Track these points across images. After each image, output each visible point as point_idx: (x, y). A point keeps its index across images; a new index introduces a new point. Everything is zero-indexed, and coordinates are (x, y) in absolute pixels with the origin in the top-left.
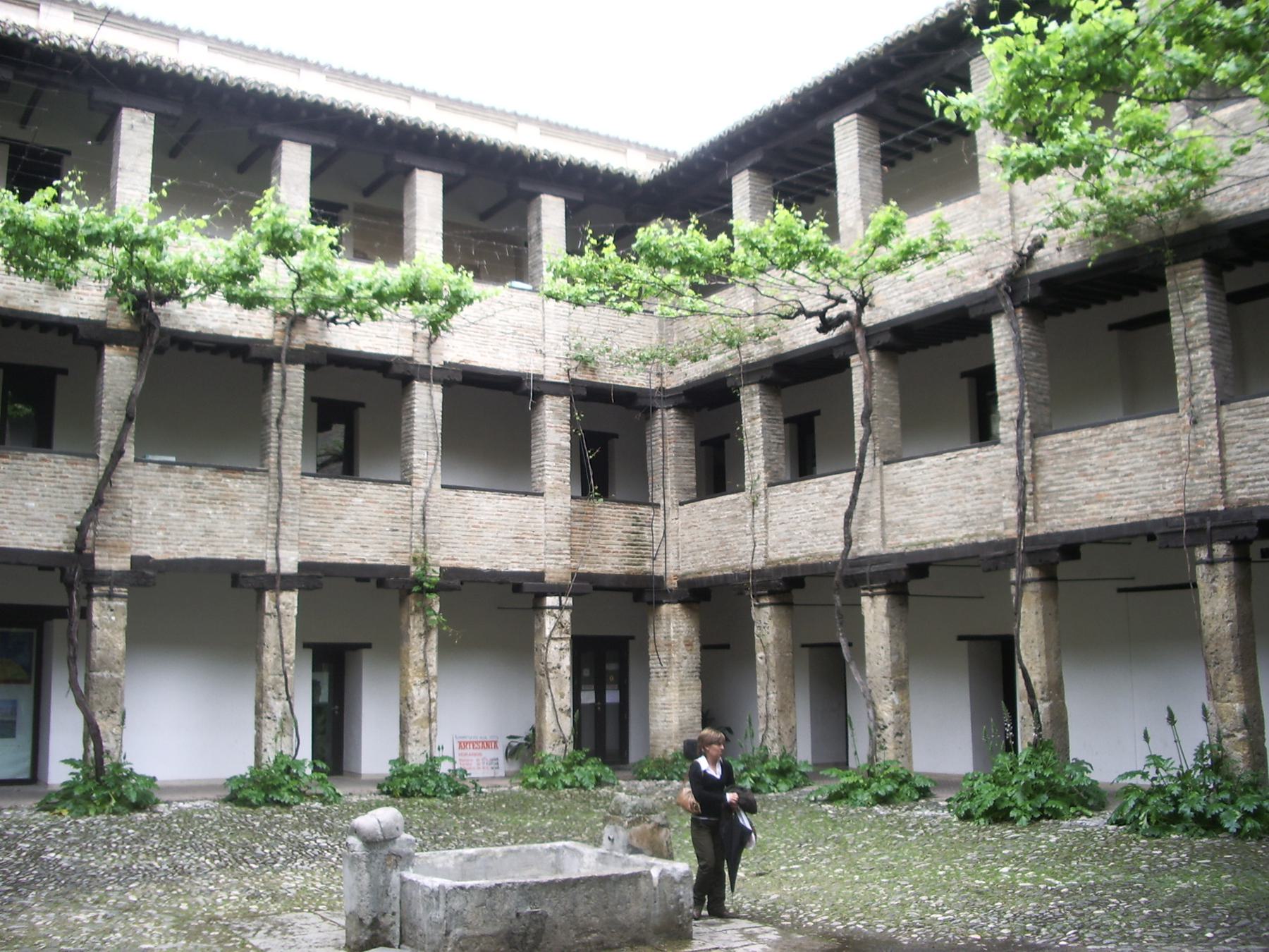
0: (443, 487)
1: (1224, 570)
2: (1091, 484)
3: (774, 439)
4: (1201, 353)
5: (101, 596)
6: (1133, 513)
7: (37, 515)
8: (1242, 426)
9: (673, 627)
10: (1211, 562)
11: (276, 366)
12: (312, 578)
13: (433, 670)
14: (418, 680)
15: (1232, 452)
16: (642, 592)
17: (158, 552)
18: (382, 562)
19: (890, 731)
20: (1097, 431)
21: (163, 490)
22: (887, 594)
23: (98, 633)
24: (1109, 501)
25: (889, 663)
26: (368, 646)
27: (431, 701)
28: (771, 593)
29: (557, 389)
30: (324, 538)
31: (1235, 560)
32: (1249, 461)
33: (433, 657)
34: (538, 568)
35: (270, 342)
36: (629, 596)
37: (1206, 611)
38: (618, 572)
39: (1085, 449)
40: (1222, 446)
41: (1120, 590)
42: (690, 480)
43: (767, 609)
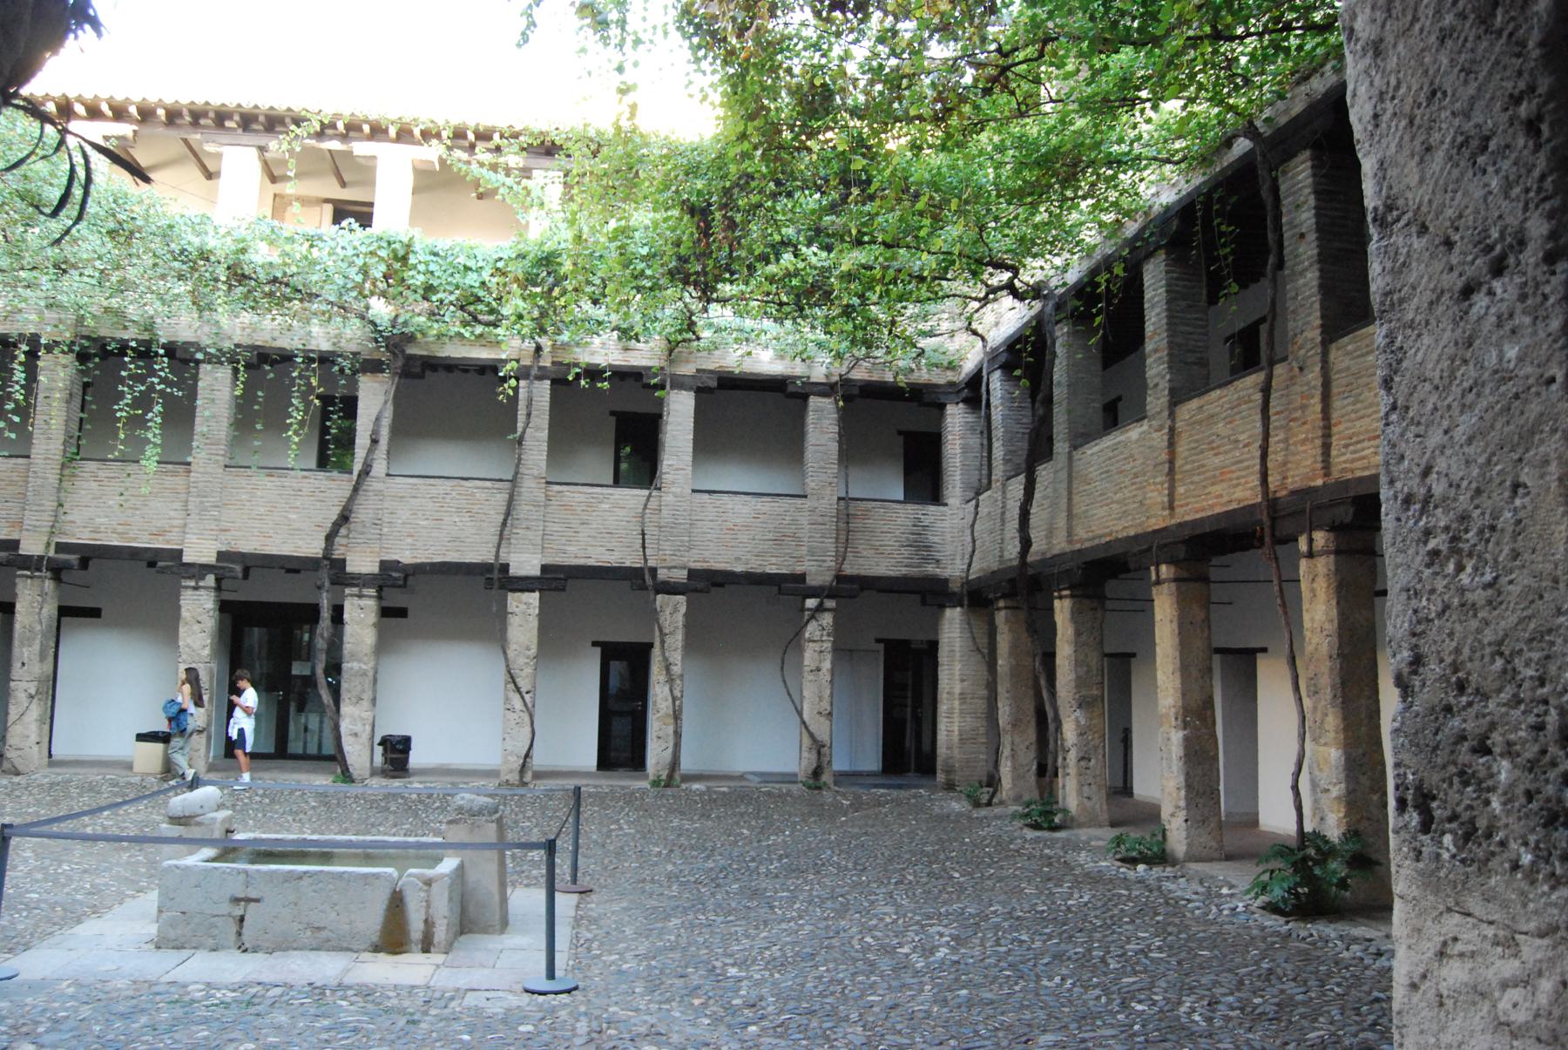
0: (694, 491)
3: (1018, 428)
7: (296, 525)
9: (953, 628)
13: (676, 669)
17: (407, 557)
18: (628, 564)
20: (1224, 391)
22: (1072, 596)
23: (349, 630)
25: (1072, 676)
27: (674, 699)
28: (1004, 596)
29: (827, 389)
31: (1337, 552)
33: (676, 657)
34: (799, 569)
36: (918, 597)
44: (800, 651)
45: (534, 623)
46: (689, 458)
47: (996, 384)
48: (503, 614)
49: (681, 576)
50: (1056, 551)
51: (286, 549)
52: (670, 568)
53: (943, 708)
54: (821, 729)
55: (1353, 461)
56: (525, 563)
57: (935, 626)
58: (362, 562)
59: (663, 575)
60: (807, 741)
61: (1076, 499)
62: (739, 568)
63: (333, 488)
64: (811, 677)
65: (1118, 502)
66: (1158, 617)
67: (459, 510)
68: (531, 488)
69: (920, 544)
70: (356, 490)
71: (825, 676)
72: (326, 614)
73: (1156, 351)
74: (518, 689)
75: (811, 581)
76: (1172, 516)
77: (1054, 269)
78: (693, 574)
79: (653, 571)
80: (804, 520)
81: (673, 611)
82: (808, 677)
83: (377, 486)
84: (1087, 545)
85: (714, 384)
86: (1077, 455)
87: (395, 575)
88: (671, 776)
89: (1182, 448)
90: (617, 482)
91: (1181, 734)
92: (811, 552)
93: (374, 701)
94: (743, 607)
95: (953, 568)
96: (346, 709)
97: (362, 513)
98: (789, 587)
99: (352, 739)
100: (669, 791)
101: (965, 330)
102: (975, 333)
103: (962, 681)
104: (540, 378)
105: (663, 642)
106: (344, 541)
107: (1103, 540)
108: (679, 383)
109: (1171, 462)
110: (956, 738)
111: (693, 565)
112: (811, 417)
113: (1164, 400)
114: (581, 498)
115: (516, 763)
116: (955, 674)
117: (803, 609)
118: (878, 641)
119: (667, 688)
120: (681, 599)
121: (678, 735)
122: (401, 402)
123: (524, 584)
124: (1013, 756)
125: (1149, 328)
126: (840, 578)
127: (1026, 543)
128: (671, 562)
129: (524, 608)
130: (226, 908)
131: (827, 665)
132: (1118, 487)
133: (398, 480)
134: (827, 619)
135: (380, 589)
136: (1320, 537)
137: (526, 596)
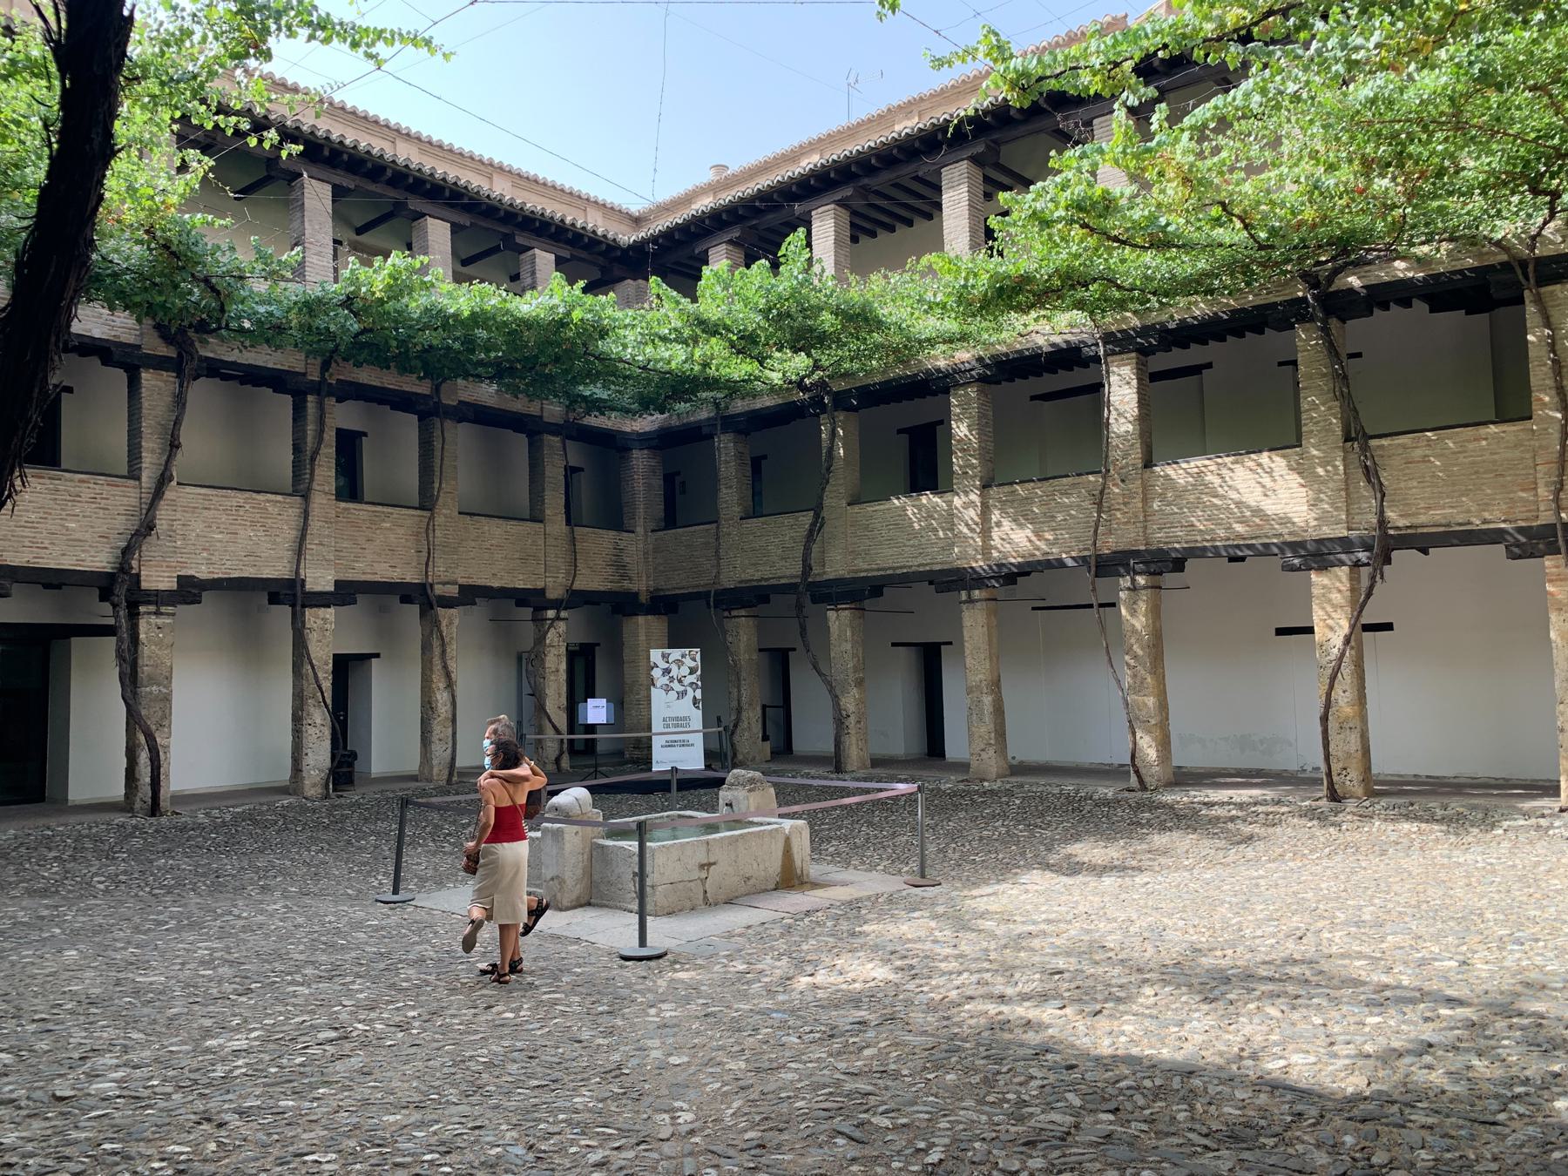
7: (77, 536)
11: (310, 398)
14: (442, 686)
17: (203, 572)
19: (852, 719)
21: (206, 513)
26: (377, 656)
30: (357, 558)
34: (540, 585)
35: (304, 374)
42: (659, 510)
47: (726, 447)
49: (453, 591)
51: (67, 563)
56: (320, 579)
58: (157, 576)
59: (439, 590)
62: (496, 584)
75: (552, 594)
95: (641, 585)
97: (161, 524)
105: (444, 652)
111: (461, 581)
121: (454, 734)
123: (321, 600)
127: (807, 568)
130: (696, 874)
133: (188, 489)
134: (562, 626)
137: (322, 612)
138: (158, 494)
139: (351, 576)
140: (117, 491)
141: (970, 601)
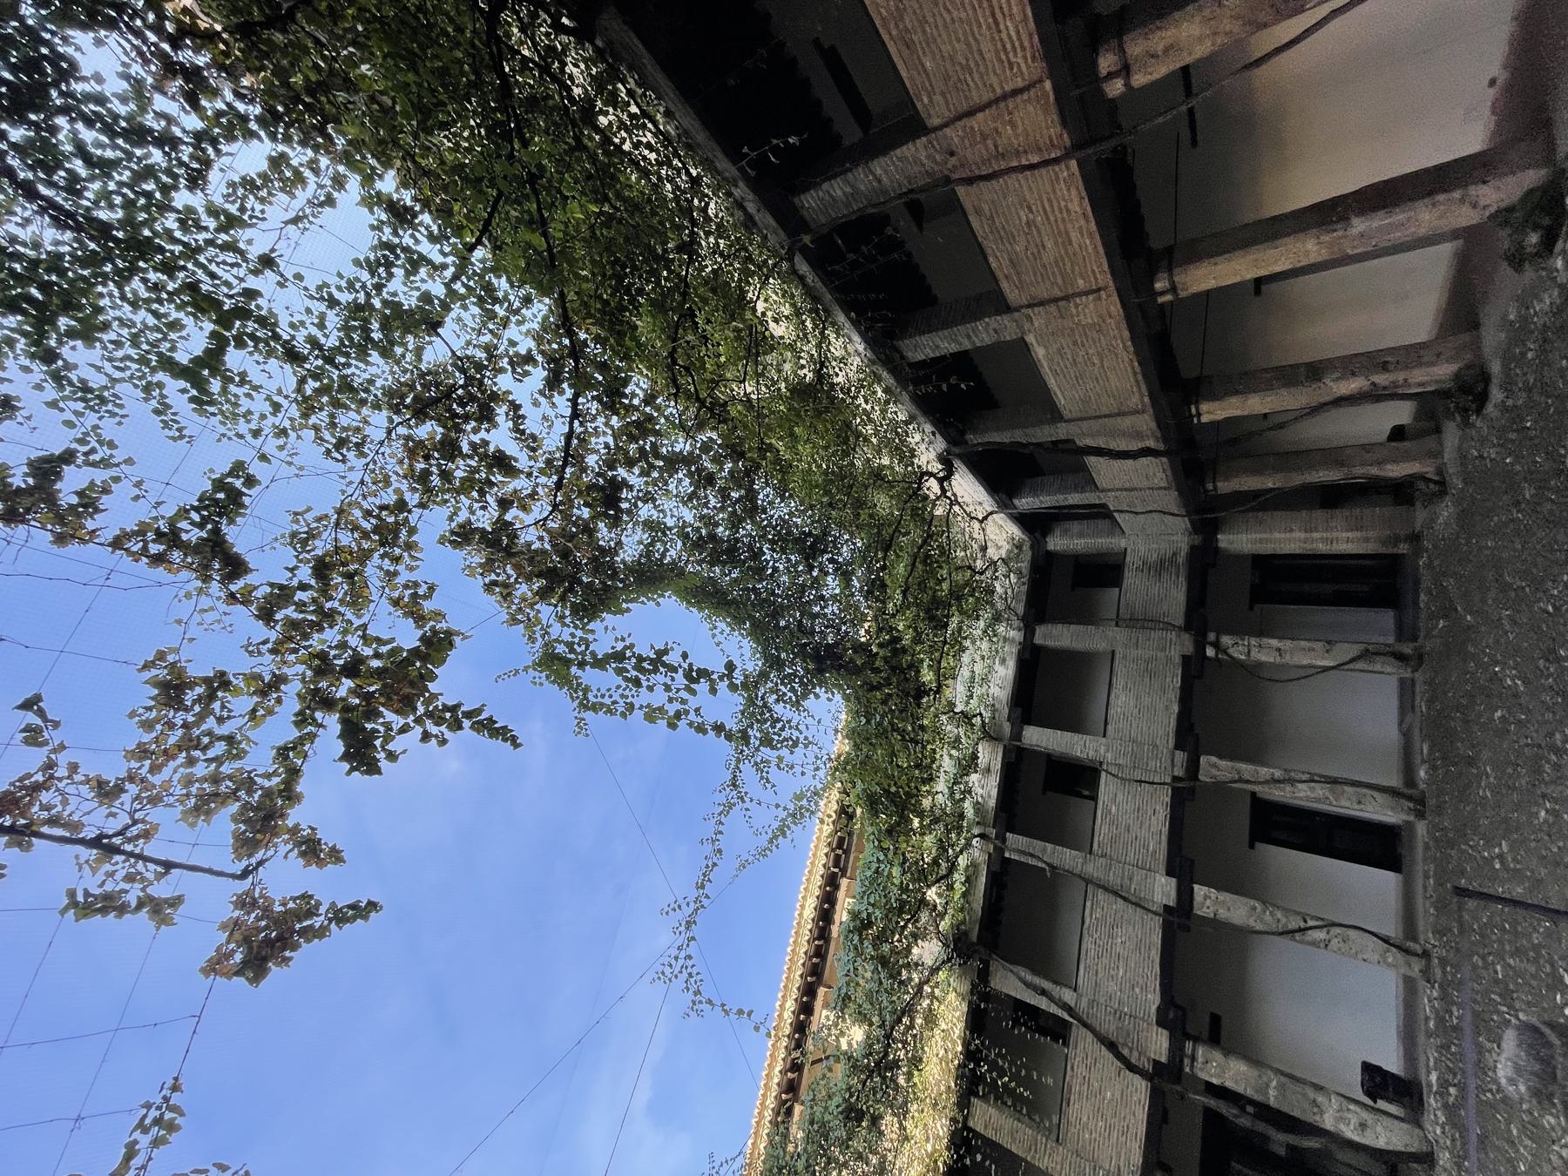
1: (1136, 47)
2: (1049, 245)
4: (879, 172)
5: (1192, 1067)
6: (1074, 192)
8: (943, 94)
9: (1240, 540)
10: (1125, 70)
12: (1181, 866)
13: (1278, 774)
14: (1288, 788)
15: (979, 96)
16: (1204, 564)
17: (1154, 999)
18: (1168, 799)
20: (989, 251)
22: (1197, 403)
23: (1229, 1084)
24: (1063, 220)
25: (1284, 392)
28: (1203, 483)
29: (1029, 630)
32: (982, 68)
33: (1265, 772)
34: (1177, 660)
37: (1201, 51)
38: (1184, 588)
39: (1011, 261)
40: (971, 113)
41: (1194, 143)
42: (1103, 524)
43: (1219, 484)
44: (1260, 664)
45: (1225, 896)
46: (1076, 737)
47: (1025, 503)
48: (1215, 923)
49: (1180, 756)
50: (1153, 425)
51: (1142, 1115)
52: (1173, 766)
53: (1322, 548)
54: (1346, 651)
55: (1023, 49)
57: (1238, 558)
59: (1179, 772)
60: (1360, 665)
61: (1105, 411)
62: (1176, 708)
63: (1083, 1046)
64: (1288, 657)
65: (1102, 361)
66: (1211, 284)
67: (1111, 936)
68: (1093, 868)
69: (1160, 567)
70: (1085, 1025)
71: (1286, 645)
72: (1212, 1103)
73: (969, 337)
74: (1300, 930)
76: (1105, 288)
77: (927, 451)
78: (1177, 747)
79: (1175, 779)
80: (1134, 653)
81: (1214, 768)
82: (1287, 659)
83: (1084, 1003)
84: (1144, 387)
85: (1019, 710)
86: (1067, 414)
87: (1171, 1015)
88: (1410, 798)
89: (1043, 292)
90: (1094, 798)
91: (1355, 221)
92: (1163, 649)
93: (1319, 1088)
94: (1214, 709)
96: (1328, 1122)
97: (1110, 1027)
98: (1194, 670)
99: (1368, 1132)
100: (1431, 802)
101: (983, 526)
102: (985, 518)
103: (1291, 530)
104: (1004, 840)
105: (1248, 782)
106: (1135, 1054)
107: (1138, 369)
108: (1017, 735)
109: (1056, 300)
110: (1358, 534)
111: (1171, 744)
112: (1050, 643)
113: (1005, 320)
114: (1105, 829)
115: (1393, 956)
116: (1288, 537)
117: (1217, 659)
118: (1251, 608)
119: (1300, 786)
120: (1203, 759)
122: (1013, 958)
123: (1185, 895)
124: (1379, 463)
125: (954, 348)
126: (1187, 627)
127: (1147, 452)
128: (1166, 762)
129: (1207, 900)
131: (1274, 642)
132: (1086, 364)
134: (1226, 640)
135: (1188, 1037)
136: (1106, 62)
138: (1080, 1020)
139: (1162, 855)
140: (1081, 1046)
141: (1173, 289)
